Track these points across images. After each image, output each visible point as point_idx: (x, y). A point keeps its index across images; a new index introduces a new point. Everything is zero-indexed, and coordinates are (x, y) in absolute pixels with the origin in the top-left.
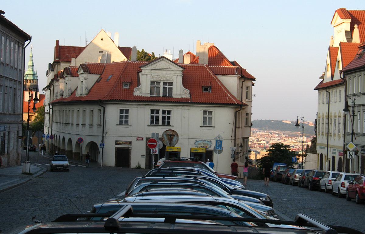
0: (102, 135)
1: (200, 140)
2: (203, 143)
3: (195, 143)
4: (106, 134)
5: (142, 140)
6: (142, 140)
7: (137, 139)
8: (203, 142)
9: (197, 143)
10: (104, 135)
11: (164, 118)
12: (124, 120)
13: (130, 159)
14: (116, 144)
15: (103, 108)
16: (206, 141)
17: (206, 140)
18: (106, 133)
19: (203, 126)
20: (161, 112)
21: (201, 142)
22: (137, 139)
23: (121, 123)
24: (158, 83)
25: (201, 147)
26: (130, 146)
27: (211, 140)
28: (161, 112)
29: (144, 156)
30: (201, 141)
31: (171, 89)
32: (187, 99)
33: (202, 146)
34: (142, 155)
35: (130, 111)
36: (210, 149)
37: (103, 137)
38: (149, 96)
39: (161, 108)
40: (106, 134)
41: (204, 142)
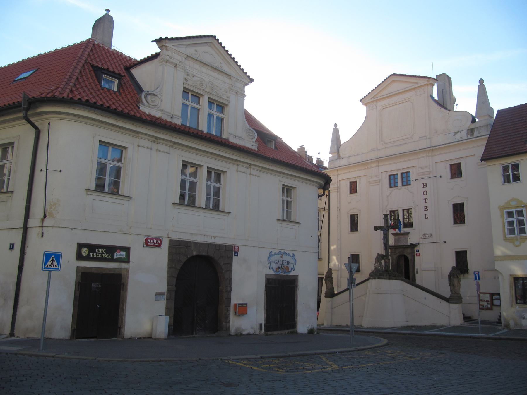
0: (22, 225)
1: (277, 251)
2: (281, 259)
3: (269, 257)
4: (43, 220)
5: (160, 245)
6: (160, 245)
7: (147, 244)
8: (281, 257)
9: (273, 258)
10: (31, 222)
11: (209, 187)
12: (108, 181)
13: (123, 310)
14: (79, 257)
15: (33, 132)
16: (286, 254)
17: (288, 252)
18: (45, 216)
19: (283, 220)
20: (203, 174)
21: (280, 256)
22: (147, 244)
23: (100, 187)
24: (197, 97)
25: (279, 268)
26: (124, 265)
27: (295, 253)
28: (203, 174)
29: (163, 297)
30: (278, 254)
31: (221, 120)
32: (255, 150)
33: (280, 267)
34: (158, 294)
35: (129, 154)
36: (292, 273)
37: (25, 229)
38: (178, 122)
39: (206, 162)
40: (43, 220)
41: (284, 256)
